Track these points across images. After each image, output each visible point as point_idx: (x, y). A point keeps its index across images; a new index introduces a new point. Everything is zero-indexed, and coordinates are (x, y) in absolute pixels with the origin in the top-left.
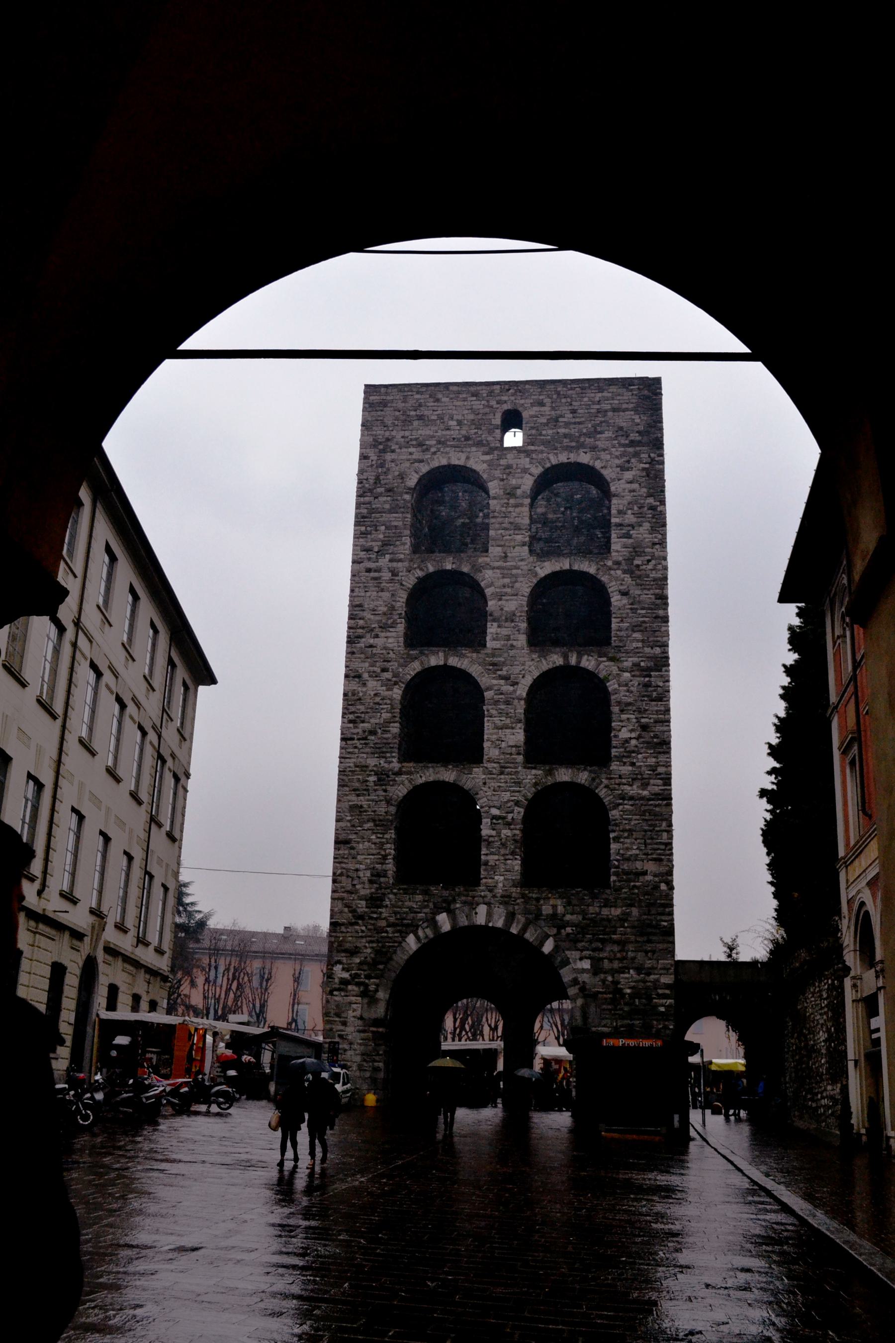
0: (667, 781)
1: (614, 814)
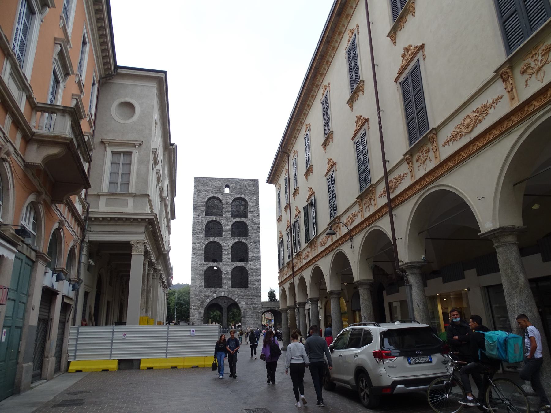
0: (260, 265)
1: (249, 272)
